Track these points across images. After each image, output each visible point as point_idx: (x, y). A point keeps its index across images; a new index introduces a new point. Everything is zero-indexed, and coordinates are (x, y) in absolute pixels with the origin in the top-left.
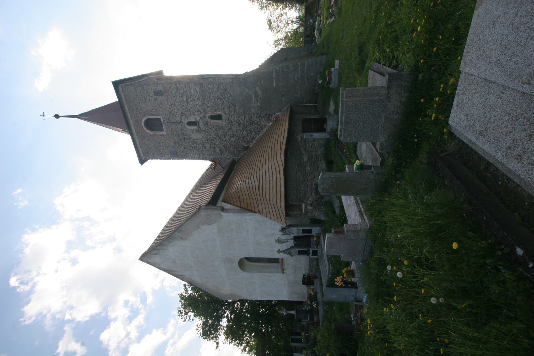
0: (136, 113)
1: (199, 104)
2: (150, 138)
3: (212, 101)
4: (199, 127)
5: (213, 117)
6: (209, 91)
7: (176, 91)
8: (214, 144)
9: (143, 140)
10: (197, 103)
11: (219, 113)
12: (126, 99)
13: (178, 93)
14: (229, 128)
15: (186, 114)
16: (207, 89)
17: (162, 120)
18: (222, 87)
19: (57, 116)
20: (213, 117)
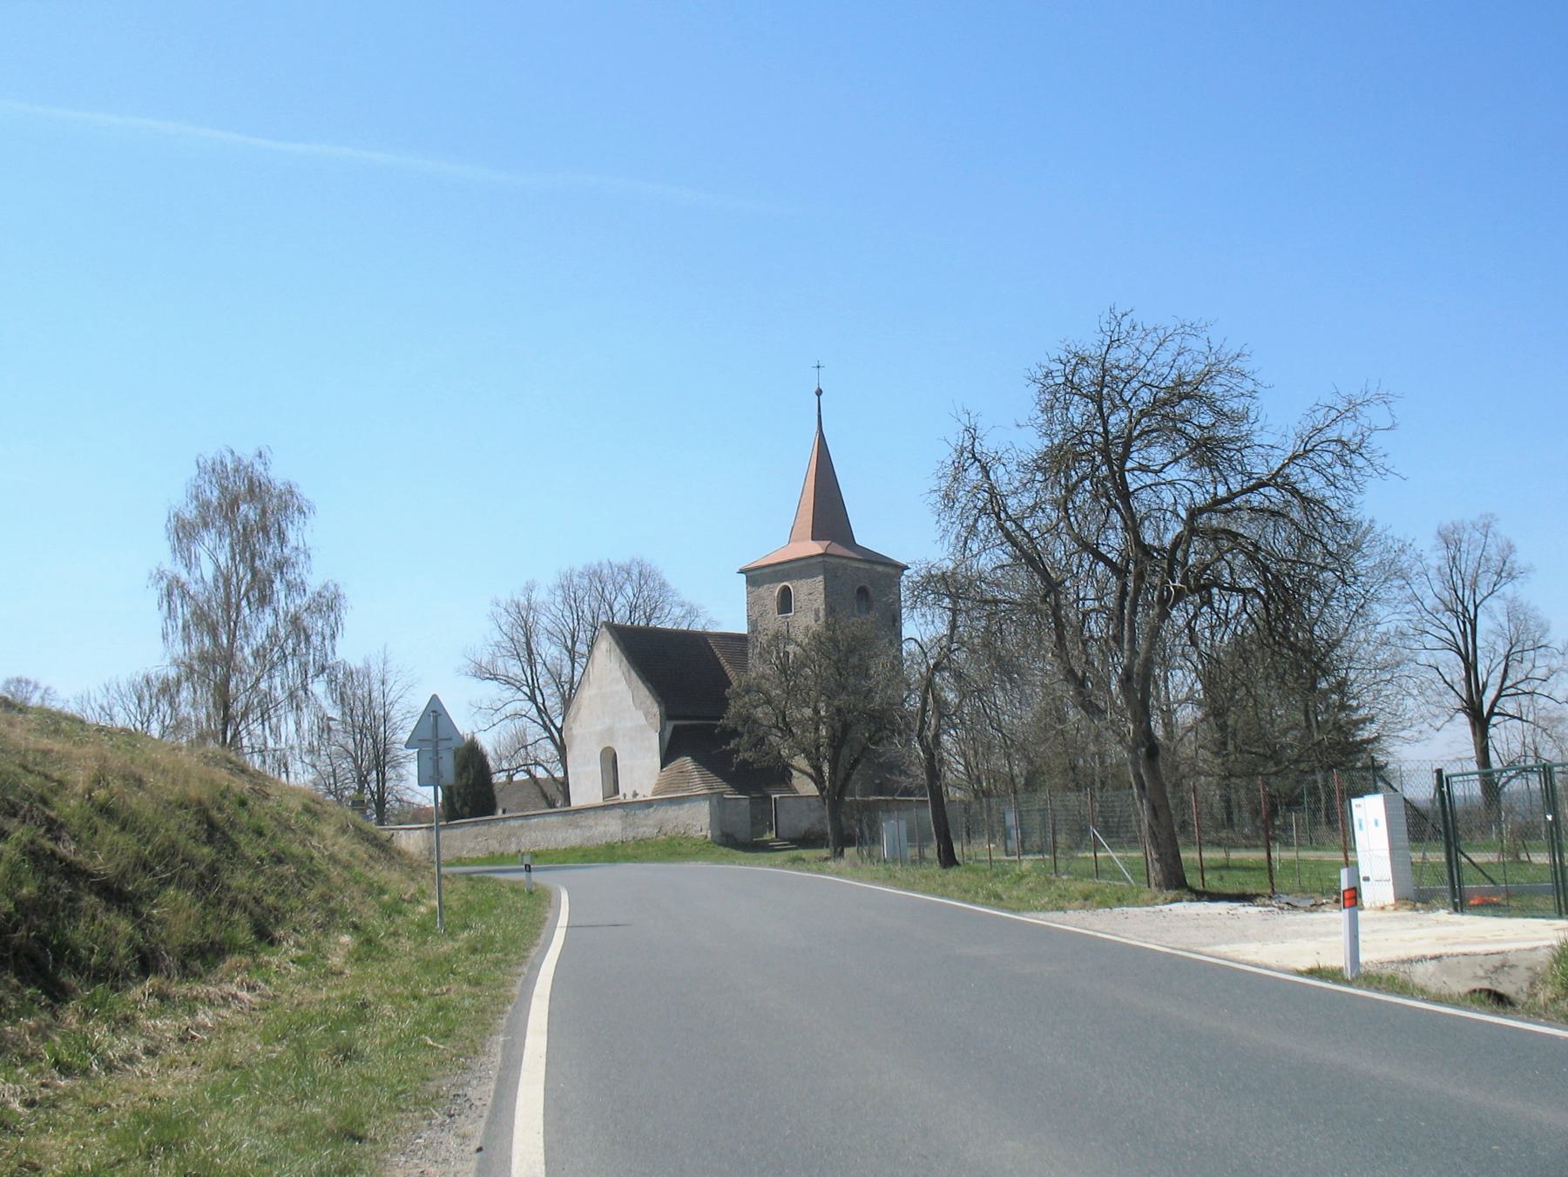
19: (819, 393)
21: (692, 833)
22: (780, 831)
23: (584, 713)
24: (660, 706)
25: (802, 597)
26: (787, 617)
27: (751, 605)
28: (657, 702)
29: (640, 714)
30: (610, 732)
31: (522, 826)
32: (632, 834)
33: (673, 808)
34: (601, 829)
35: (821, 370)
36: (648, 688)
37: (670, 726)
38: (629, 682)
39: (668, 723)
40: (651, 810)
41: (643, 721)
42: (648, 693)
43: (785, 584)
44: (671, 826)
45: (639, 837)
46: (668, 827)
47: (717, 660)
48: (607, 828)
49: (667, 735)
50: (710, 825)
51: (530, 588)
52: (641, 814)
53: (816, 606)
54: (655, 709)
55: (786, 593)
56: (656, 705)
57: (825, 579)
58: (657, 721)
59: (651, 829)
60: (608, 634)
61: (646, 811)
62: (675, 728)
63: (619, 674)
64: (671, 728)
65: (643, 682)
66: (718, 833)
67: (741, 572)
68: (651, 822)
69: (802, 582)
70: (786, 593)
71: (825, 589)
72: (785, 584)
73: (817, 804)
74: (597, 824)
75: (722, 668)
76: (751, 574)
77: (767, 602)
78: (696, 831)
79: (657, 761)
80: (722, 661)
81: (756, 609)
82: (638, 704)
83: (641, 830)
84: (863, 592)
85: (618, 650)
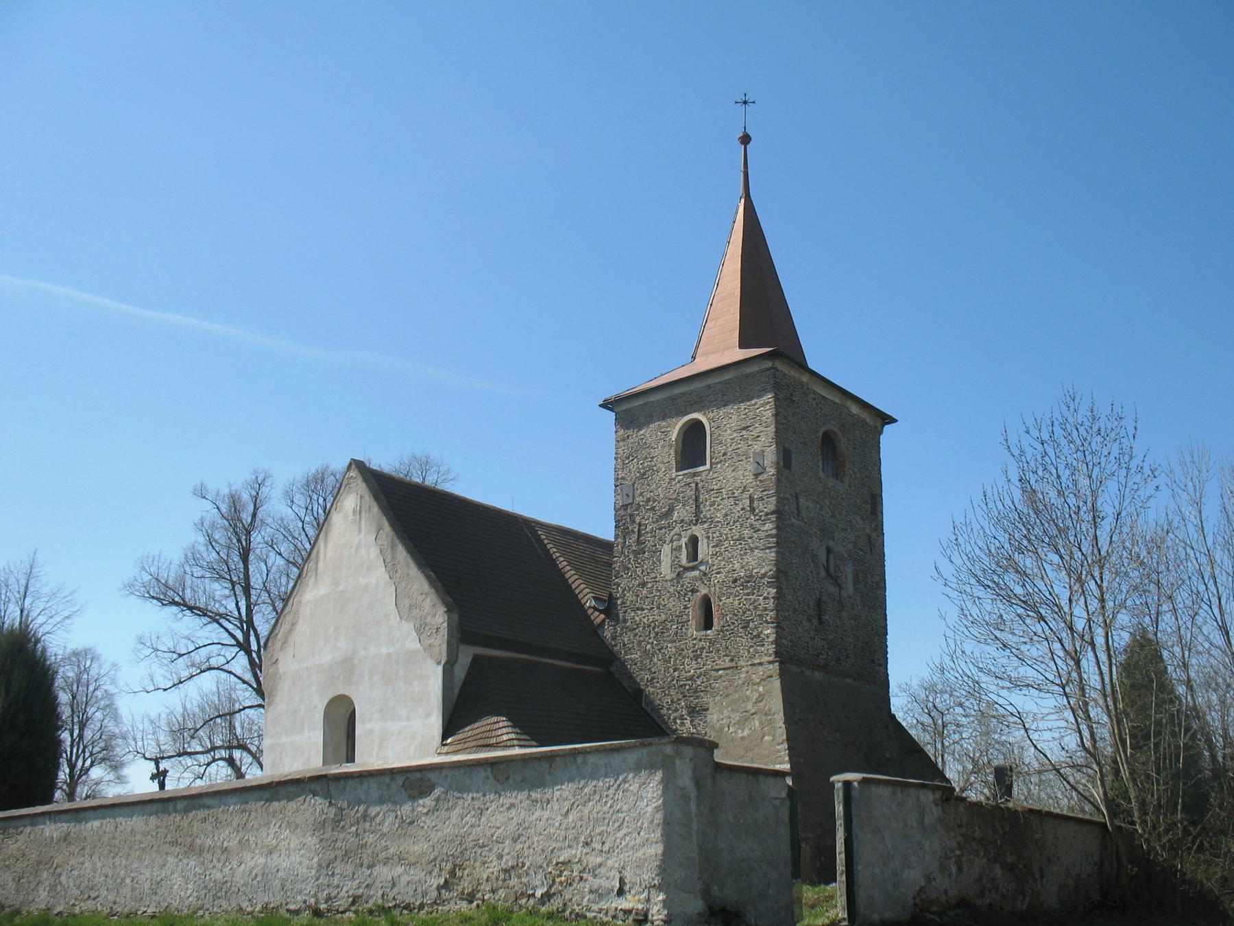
0: (717, 400)
1: (735, 570)
2: (663, 432)
3: (740, 604)
4: (687, 569)
5: (707, 605)
6: (761, 598)
7: (763, 511)
8: (648, 607)
9: (658, 413)
10: (737, 566)
11: (715, 621)
12: (747, 376)
13: (757, 517)
14: (683, 650)
15: (714, 535)
16: (765, 595)
17: (702, 468)
18: (769, 631)
19: (745, 140)
20: (707, 605)
21: (579, 898)
22: (862, 896)
23: (303, 628)
24: (449, 611)
25: (727, 436)
26: (695, 474)
27: (623, 461)
28: (445, 603)
29: (408, 627)
30: (347, 666)
31: (65, 838)
32: (350, 888)
33: (506, 800)
34: (255, 861)
35: (750, 108)
36: (428, 577)
37: (466, 655)
38: (391, 567)
39: (462, 648)
40: (428, 802)
41: (412, 643)
42: (425, 586)
43: (695, 416)
44: (495, 867)
45: (376, 898)
46: (487, 869)
47: (554, 562)
48: (275, 860)
49: (460, 672)
50: (664, 869)
51: (259, 485)
52: (386, 817)
53: (757, 447)
54: (439, 617)
55: (694, 434)
56: (441, 610)
57: (776, 399)
58: (440, 642)
59: (417, 874)
60: (360, 480)
61: (406, 808)
62: (476, 659)
63: (374, 552)
64: (469, 659)
65: (420, 566)
66: (696, 905)
67: (607, 405)
68: (418, 848)
69: (729, 409)
70: (694, 434)
71: (776, 415)
72: (695, 416)
73: (937, 812)
74: (244, 844)
75: (563, 575)
76: (626, 406)
77: (655, 452)
78: (599, 894)
79: (436, 723)
80: (563, 564)
81: (633, 466)
82: (405, 609)
83: (384, 873)
84: (828, 442)
85: (376, 509)
